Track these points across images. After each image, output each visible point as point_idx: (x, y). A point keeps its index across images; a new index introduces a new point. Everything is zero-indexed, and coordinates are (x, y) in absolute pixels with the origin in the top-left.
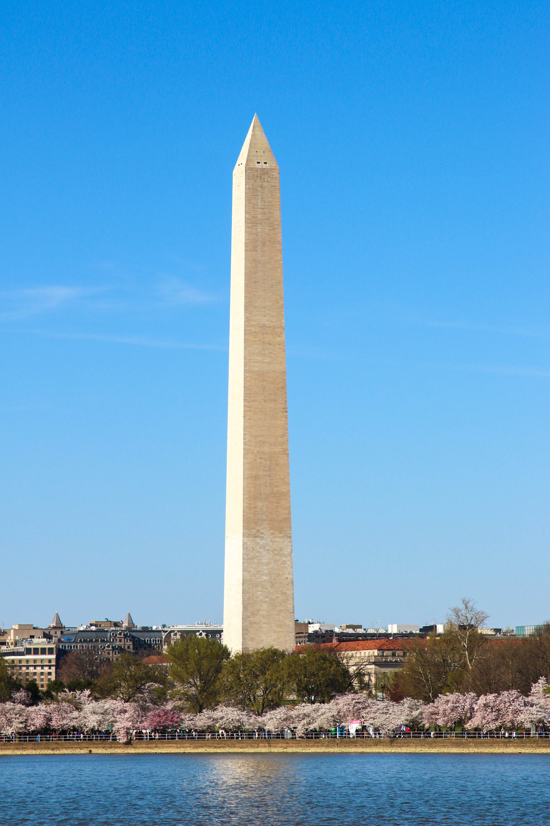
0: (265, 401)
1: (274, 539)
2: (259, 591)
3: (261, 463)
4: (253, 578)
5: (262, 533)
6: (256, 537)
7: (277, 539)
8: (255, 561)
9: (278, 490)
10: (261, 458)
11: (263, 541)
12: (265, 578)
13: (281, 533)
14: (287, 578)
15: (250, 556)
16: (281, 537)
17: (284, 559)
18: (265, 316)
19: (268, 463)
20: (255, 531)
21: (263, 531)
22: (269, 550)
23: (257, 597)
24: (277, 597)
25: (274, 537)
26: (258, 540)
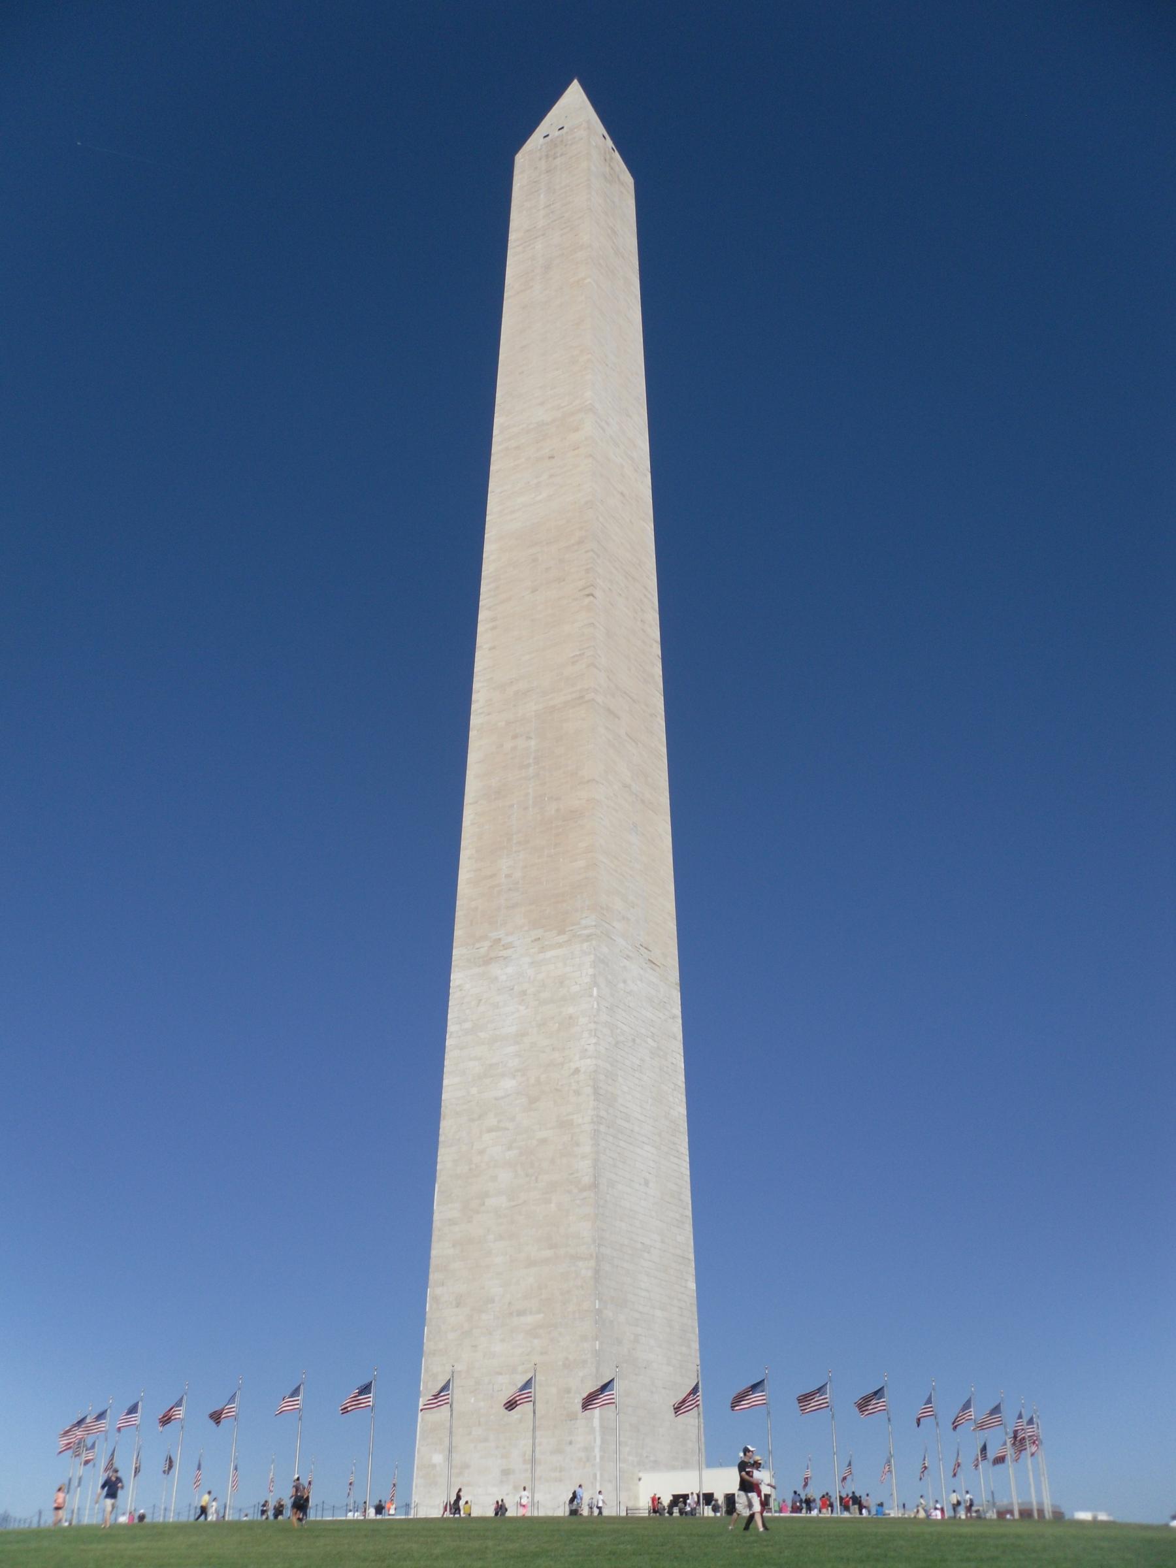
0: (534, 590)
1: (541, 956)
2: (490, 1130)
3: (514, 748)
4: (474, 1090)
5: (505, 947)
6: (487, 961)
7: (549, 954)
8: (482, 1035)
9: (558, 810)
10: (515, 737)
11: (510, 970)
12: (509, 1084)
13: (562, 932)
14: (577, 1071)
15: (468, 1025)
16: (560, 945)
17: (571, 1010)
18: (542, 404)
19: (533, 743)
20: (487, 944)
21: (510, 939)
22: (524, 993)
23: (482, 1152)
24: (544, 1141)
25: (542, 950)
26: (495, 970)
